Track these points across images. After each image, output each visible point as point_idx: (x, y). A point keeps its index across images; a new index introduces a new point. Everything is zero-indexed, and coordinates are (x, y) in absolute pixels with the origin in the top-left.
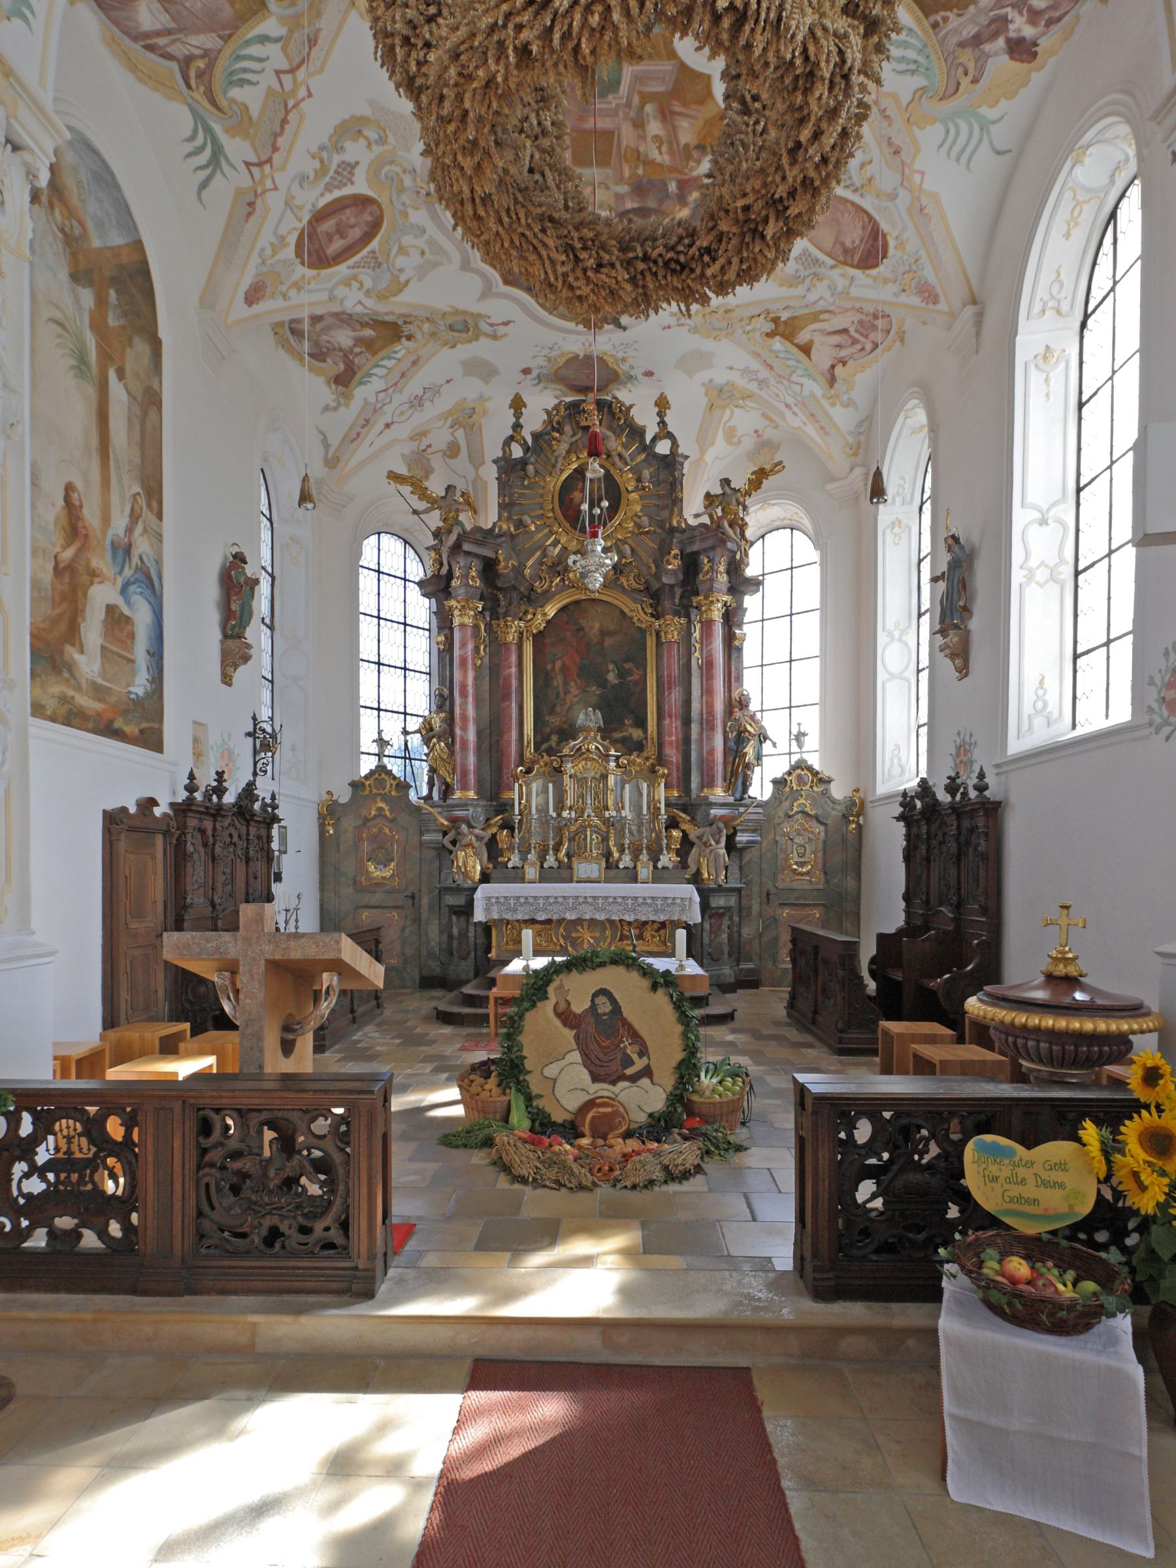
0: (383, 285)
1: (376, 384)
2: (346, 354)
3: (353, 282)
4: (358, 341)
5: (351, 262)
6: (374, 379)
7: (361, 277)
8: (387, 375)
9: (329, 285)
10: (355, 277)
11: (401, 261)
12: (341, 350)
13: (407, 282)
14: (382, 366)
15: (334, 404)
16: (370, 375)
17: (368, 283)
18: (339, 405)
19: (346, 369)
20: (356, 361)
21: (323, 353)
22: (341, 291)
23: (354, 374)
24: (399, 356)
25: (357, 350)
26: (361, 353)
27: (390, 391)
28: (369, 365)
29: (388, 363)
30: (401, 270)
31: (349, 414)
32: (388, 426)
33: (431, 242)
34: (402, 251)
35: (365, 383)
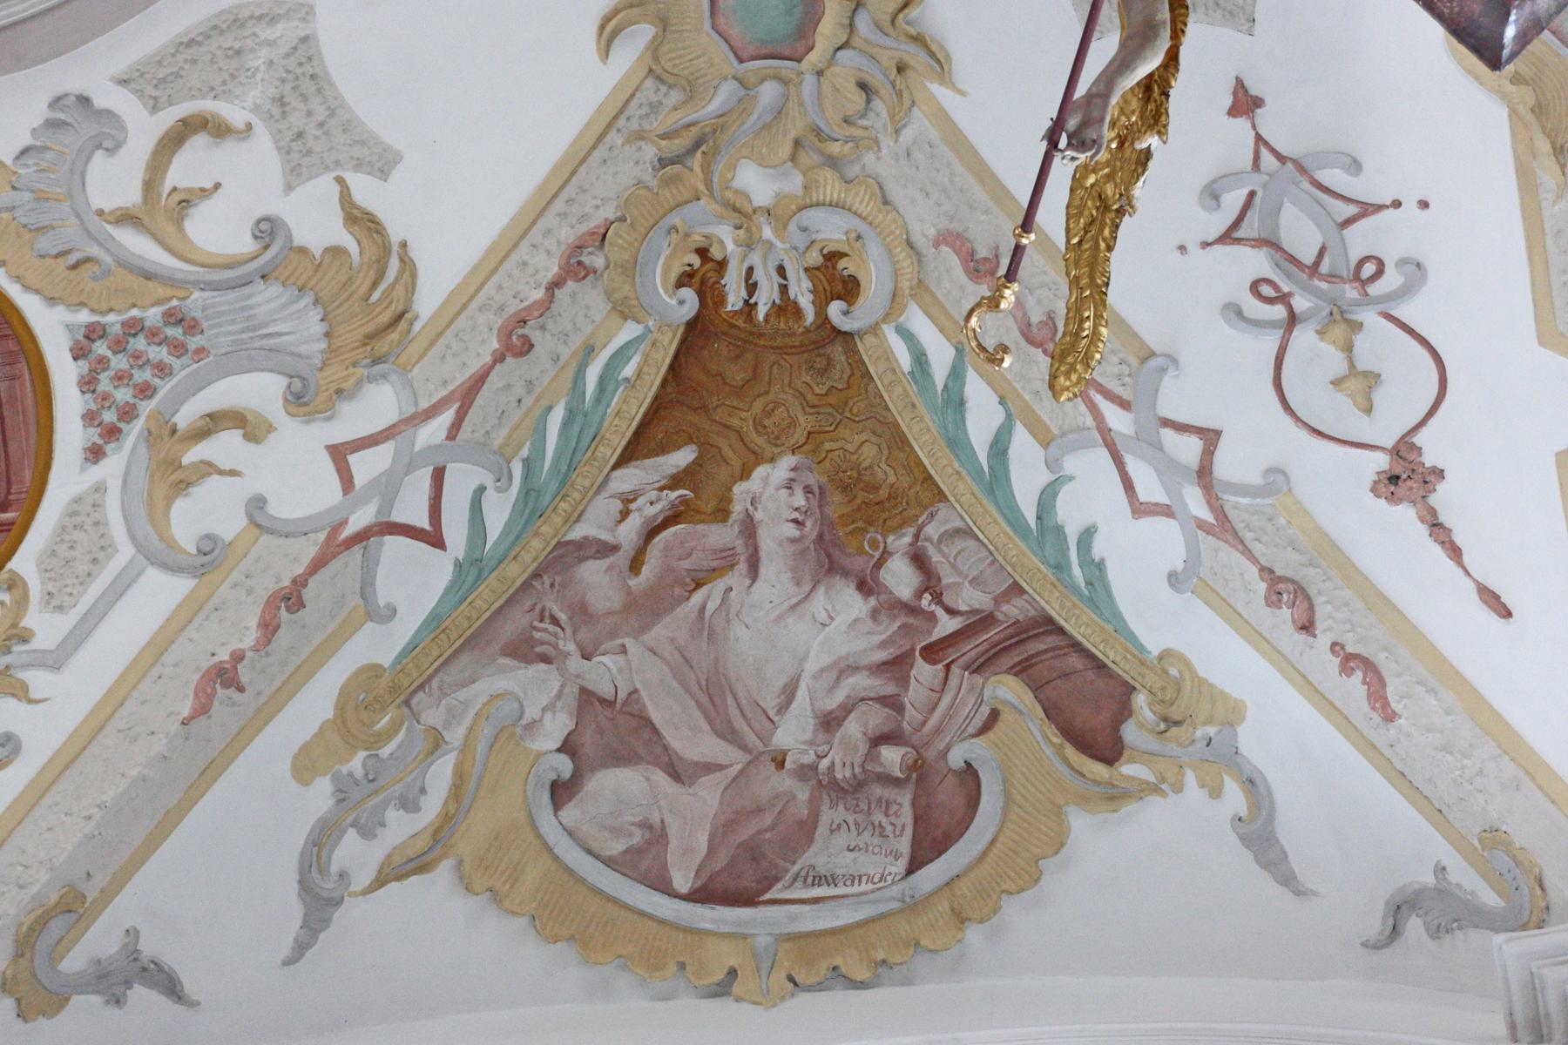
0: (305, 329)
1: (1091, 498)
2: (927, 642)
3: (195, 454)
4: (833, 554)
5: (70, 433)
6: (1070, 514)
7: (185, 417)
8: (1045, 439)
9: (125, 551)
10: (165, 434)
11: (219, 231)
12: (897, 666)
13: (360, 220)
14: (1000, 447)
15: (1235, 798)
16: (1048, 527)
17: (259, 390)
18: (1232, 761)
19: (1021, 670)
20: (971, 598)
21: (920, 772)
22: (202, 514)
23: (1049, 626)
24: (941, 356)
25: (900, 578)
26: (919, 560)
27: (1117, 420)
28: (995, 529)
29: (982, 415)
30: (268, 229)
31: (1279, 714)
32: (1406, 476)
33: (148, 81)
34: (164, 208)
35: (1096, 570)
